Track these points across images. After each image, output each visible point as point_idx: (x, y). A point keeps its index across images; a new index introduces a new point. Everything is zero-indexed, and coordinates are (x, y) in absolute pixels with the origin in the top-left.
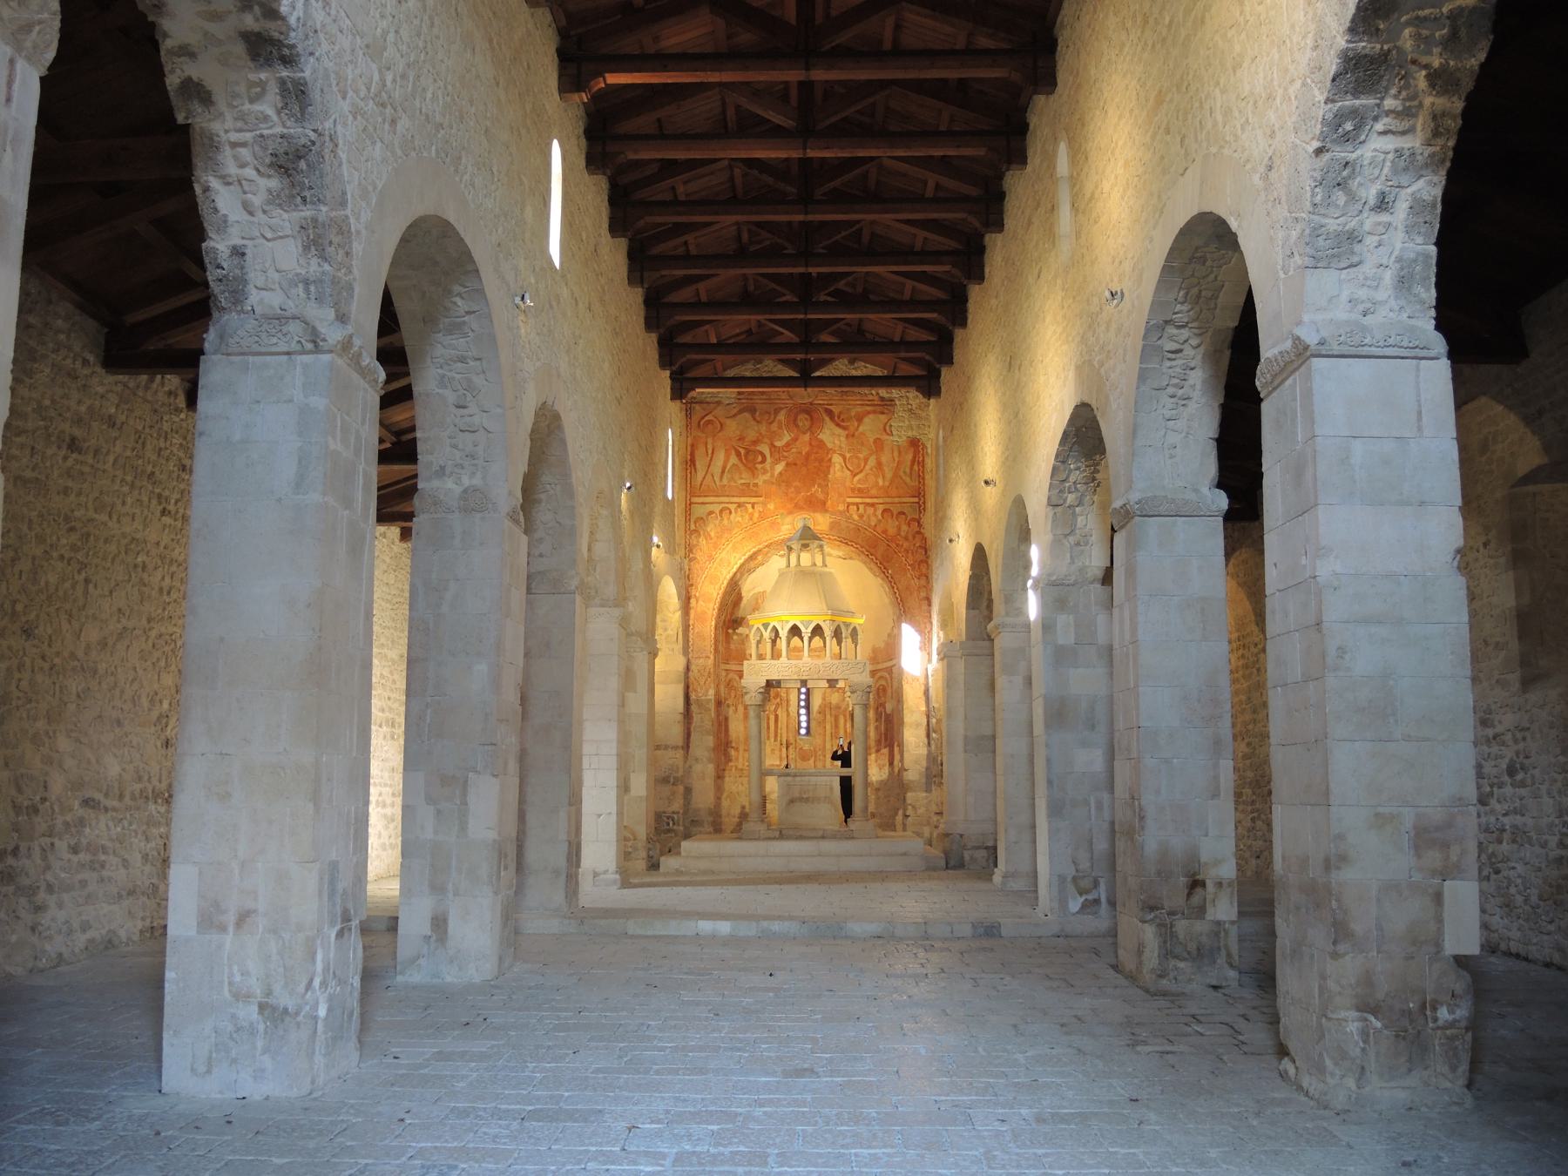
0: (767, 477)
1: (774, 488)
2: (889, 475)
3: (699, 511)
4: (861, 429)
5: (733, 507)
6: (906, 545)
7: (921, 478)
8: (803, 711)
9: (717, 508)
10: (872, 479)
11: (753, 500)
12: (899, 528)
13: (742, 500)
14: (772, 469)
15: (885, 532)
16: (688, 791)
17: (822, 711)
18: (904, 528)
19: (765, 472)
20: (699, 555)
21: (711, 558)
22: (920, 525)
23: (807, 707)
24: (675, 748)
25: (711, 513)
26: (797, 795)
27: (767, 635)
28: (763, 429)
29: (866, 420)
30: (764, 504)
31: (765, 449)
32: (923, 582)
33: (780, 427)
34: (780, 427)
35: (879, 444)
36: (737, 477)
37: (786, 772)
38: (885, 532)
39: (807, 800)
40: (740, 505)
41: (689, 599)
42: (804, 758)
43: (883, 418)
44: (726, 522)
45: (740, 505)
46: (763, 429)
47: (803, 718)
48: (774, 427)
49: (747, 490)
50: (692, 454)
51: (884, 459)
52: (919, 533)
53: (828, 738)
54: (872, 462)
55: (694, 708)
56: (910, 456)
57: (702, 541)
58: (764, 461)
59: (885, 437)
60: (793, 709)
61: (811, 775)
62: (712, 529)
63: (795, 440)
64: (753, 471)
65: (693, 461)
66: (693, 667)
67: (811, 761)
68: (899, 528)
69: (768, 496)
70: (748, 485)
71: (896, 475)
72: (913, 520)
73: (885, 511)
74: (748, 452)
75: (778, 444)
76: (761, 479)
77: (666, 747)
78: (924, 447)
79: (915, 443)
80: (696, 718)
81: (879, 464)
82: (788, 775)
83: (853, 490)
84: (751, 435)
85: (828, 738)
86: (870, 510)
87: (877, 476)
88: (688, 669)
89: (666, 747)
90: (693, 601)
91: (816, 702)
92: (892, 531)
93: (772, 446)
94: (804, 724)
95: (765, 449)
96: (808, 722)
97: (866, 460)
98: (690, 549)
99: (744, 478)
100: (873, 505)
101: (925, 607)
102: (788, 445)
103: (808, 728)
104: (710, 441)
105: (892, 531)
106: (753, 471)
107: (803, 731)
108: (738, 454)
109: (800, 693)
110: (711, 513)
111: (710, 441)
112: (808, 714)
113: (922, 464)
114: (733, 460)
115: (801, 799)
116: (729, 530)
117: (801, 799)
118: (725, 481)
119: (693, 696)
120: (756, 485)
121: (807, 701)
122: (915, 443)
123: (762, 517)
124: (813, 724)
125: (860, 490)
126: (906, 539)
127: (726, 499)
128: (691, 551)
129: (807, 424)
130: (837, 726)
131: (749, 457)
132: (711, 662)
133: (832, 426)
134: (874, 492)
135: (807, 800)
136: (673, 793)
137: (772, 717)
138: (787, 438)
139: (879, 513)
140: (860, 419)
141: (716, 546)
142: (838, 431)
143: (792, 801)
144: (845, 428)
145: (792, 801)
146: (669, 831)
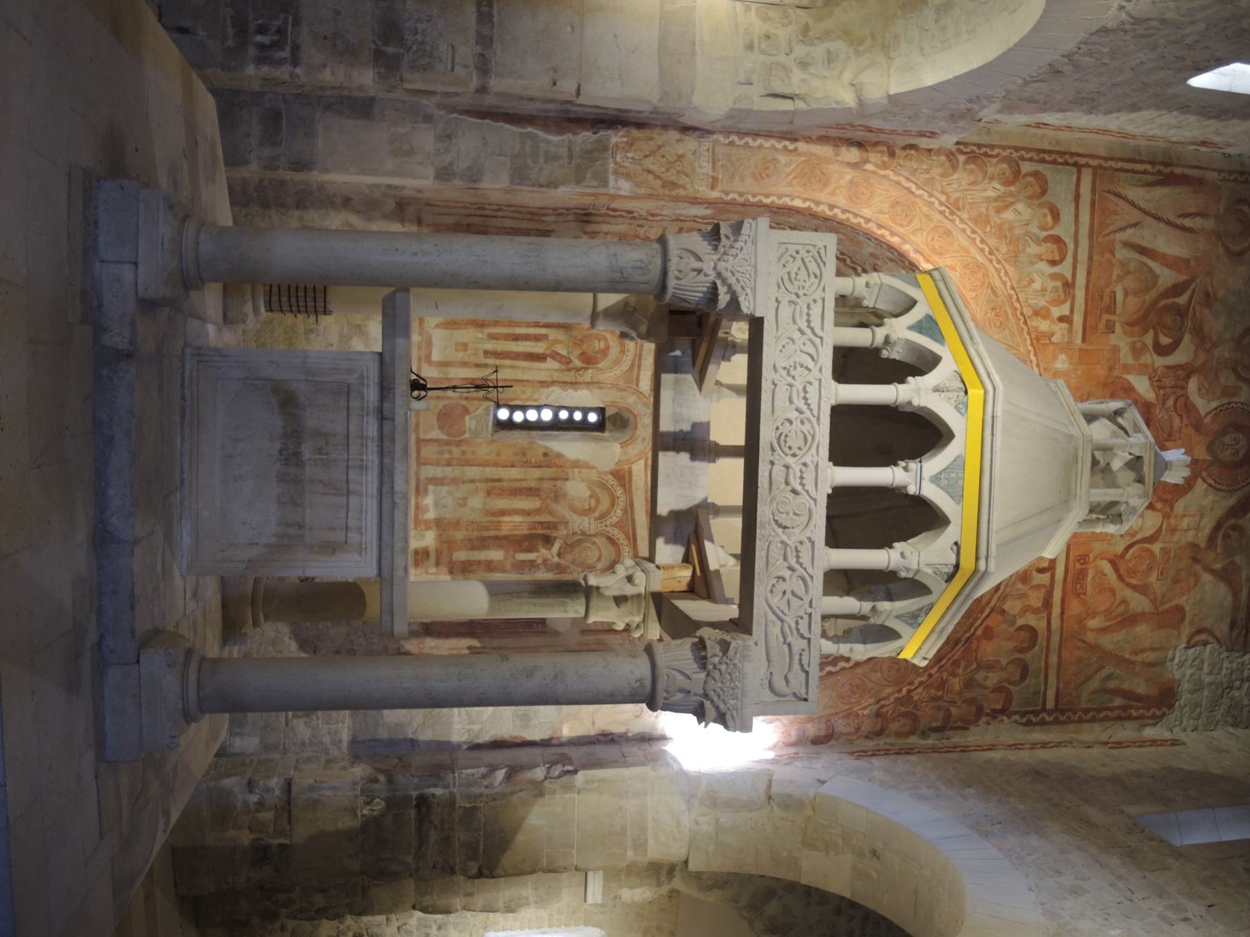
0: (1126, 356)
1: (1101, 371)
2: (1107, 641)
3: (1061, 184)
4: (1207, 577)
5: (1065, 269)
6: (956, 683)
7: (1097, 714)
8: (547, 415)
9: (1064, 230)
10: (1103, 602)
11: (1078, 319)
12: (991, 667)
13: (1080, 294)
14: (1143, 370)
15: (988, 634)
16: (363, 108)
17: (549, 459)
18: (993, 679)
19: (1136, 352)
20: (961, 178)
21: (954, 207)
22: (994, 714)
23: (556, 425)
24: (484, 68)
25: (1056, 216)
26: (311, 420)
27: (900, 333)
28: (1224, 352)
29: (1223, 589)
30: (1066, 347)
31: (1180, 357)
32: (867, 727)
33: (1226, 391)
34: (1226, 391)
35: (1171, 617)
36: (1130, 283)
37: (394, 381)
38: (988, 634)
39: (291, 457)
40: (1069, 286)
41: (860, 145)
42: (445, 418)
43: (1223, 628)
44: (1033, 249)
45: (1069, 286)
46: (1224, 352)
47: (532, 415)
48: (1227, 378)
49: (1099, 310)
50: (1183, 180)
51: (1141, 629)
52: (980, 712)
53: (490, 472)
54: (1139, 603)
55: (586, 137)
56: (1141, 689)
57: (993, 189)
58: (1161, 350)
59: (1186, 630)
60: (557, 395)
61: (385, 474)
62: (1021, 213)
63: (1198, 427)
64: (1141, 322)
65: (1168, 180)
66: (690, 143)
67: (436, 434)
68: (991, 667)
69: (1083, 356)
70: (1111, 309)
71: (1107, 656)
72: (1008, 701)
73: (1032, 631)
74: (1181, 312)
75: (1193, 385)
76: (1120, 340)
77: (485, 40)
78: (1156, 720)
79: (1166, 697)
80: (556, 141)
81: (1131, 619)
82: (385, 388)
83: (1083, 559)
84: (1215, 324)
85: (490, 472)
86: (1036, 600)
87: (1107, 612)
88: (686, 129)
89: (485, 40)
90: (853, 154)
91: (570, 447)
92: (988, 650)
93: (1188, 371)
94: (518, 417)
95: (1180, 357)
96: (526, 426)
97: (1142, 589)
98: (975, 154)
99: (1127, 305)
100: (1047, 604)
101: (812, 730)
102: (1189, 408)
103: (510, 425)
104: (1209, 224)
105: (988, 650)
106: (1141, 322)
107: (503, 414)
108: (1177, 290)
109: (585, 411)
110: (1056, 216)
111: (1209, 224)
112: (539, 426)
113: (1123, 717)
114: (1167, 277)
115: (293, 435)
116: (1014, 258)
117: (293, 435)
118: (1122, 254)
119: (616, 138)
120: (1110, 328)
121: (570, 425)
122: (1166, 697)
123: (1040, 341)
124: (518, 437)
125: (1082, 573)
126: (969, 684)
127: (1083, 255)
128: (973, 158)
129: (1226, 455)
130: (516, 492)
131: (1166, 317)
132: (704, 191)
133: (1219, 512)
134: (1075, 607)
135: (291, 457)
136: (350, 53)
137: (539, 348)
138: (1204, 405)
139: (1031, 620)
140: (1226, 575)
141: (981, 221)
142: (1208, 524)
143: (287, 401)
144: (1211, 540)
145: (287, 401)
146: (242, 32)
